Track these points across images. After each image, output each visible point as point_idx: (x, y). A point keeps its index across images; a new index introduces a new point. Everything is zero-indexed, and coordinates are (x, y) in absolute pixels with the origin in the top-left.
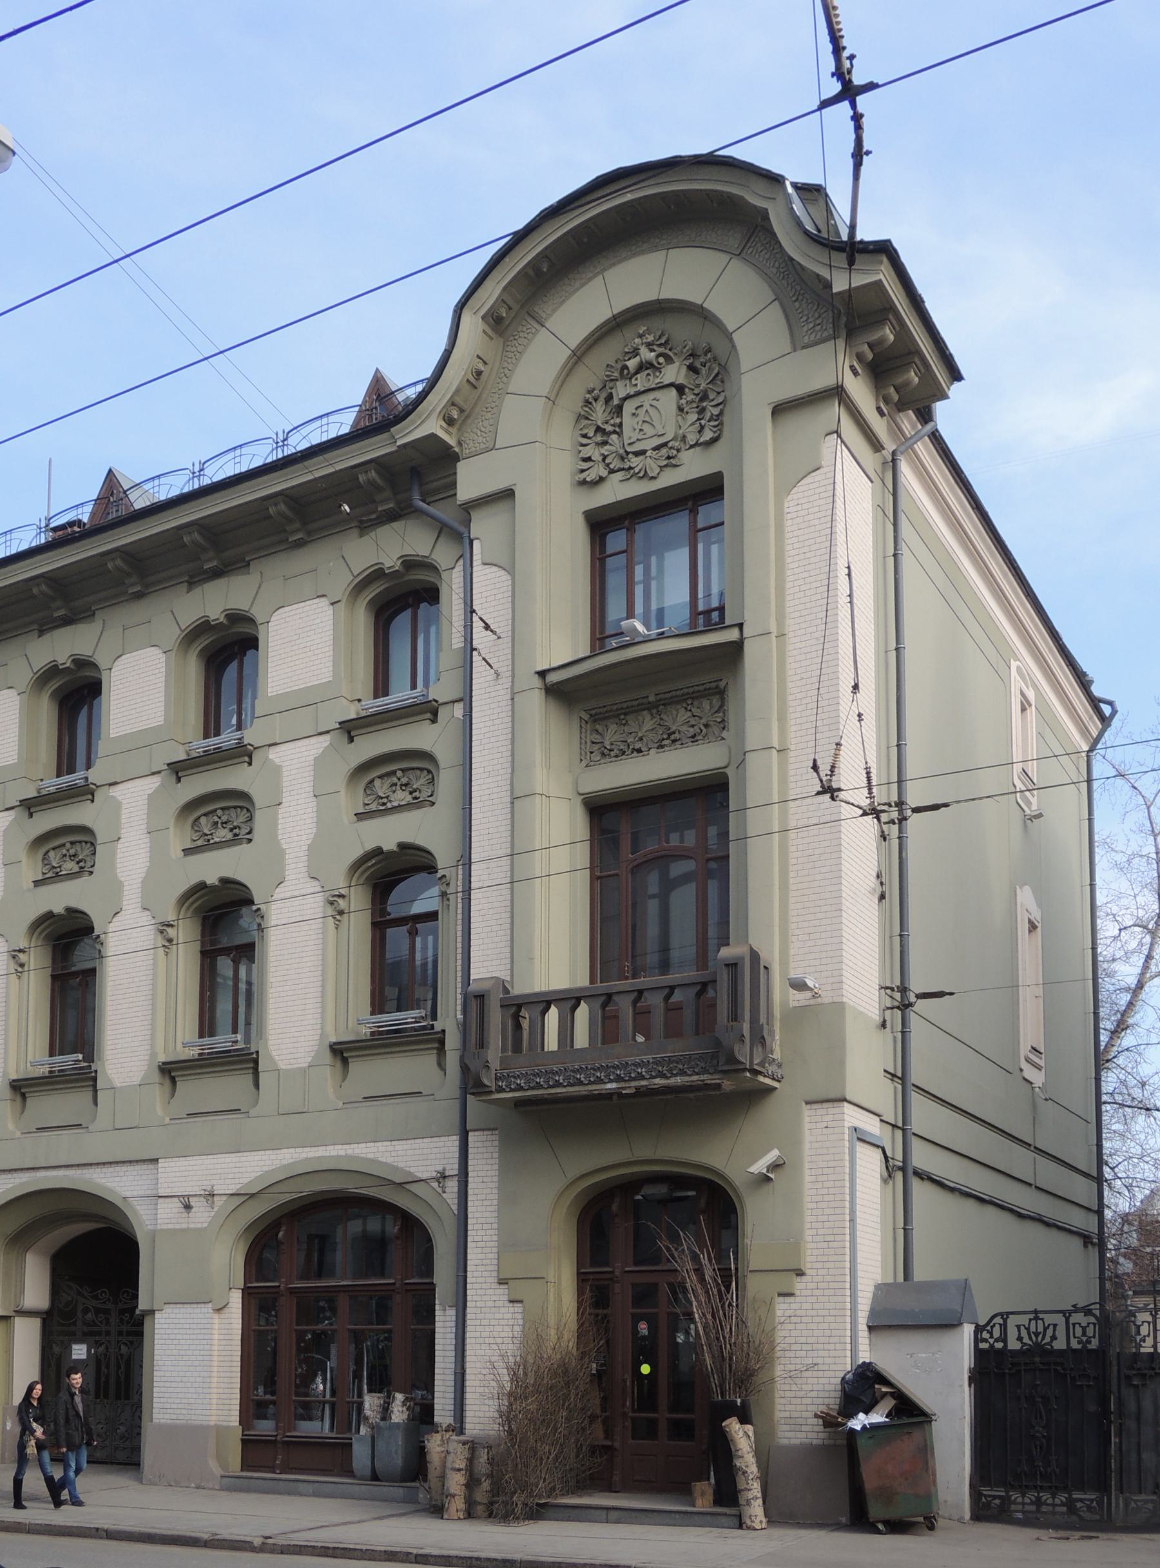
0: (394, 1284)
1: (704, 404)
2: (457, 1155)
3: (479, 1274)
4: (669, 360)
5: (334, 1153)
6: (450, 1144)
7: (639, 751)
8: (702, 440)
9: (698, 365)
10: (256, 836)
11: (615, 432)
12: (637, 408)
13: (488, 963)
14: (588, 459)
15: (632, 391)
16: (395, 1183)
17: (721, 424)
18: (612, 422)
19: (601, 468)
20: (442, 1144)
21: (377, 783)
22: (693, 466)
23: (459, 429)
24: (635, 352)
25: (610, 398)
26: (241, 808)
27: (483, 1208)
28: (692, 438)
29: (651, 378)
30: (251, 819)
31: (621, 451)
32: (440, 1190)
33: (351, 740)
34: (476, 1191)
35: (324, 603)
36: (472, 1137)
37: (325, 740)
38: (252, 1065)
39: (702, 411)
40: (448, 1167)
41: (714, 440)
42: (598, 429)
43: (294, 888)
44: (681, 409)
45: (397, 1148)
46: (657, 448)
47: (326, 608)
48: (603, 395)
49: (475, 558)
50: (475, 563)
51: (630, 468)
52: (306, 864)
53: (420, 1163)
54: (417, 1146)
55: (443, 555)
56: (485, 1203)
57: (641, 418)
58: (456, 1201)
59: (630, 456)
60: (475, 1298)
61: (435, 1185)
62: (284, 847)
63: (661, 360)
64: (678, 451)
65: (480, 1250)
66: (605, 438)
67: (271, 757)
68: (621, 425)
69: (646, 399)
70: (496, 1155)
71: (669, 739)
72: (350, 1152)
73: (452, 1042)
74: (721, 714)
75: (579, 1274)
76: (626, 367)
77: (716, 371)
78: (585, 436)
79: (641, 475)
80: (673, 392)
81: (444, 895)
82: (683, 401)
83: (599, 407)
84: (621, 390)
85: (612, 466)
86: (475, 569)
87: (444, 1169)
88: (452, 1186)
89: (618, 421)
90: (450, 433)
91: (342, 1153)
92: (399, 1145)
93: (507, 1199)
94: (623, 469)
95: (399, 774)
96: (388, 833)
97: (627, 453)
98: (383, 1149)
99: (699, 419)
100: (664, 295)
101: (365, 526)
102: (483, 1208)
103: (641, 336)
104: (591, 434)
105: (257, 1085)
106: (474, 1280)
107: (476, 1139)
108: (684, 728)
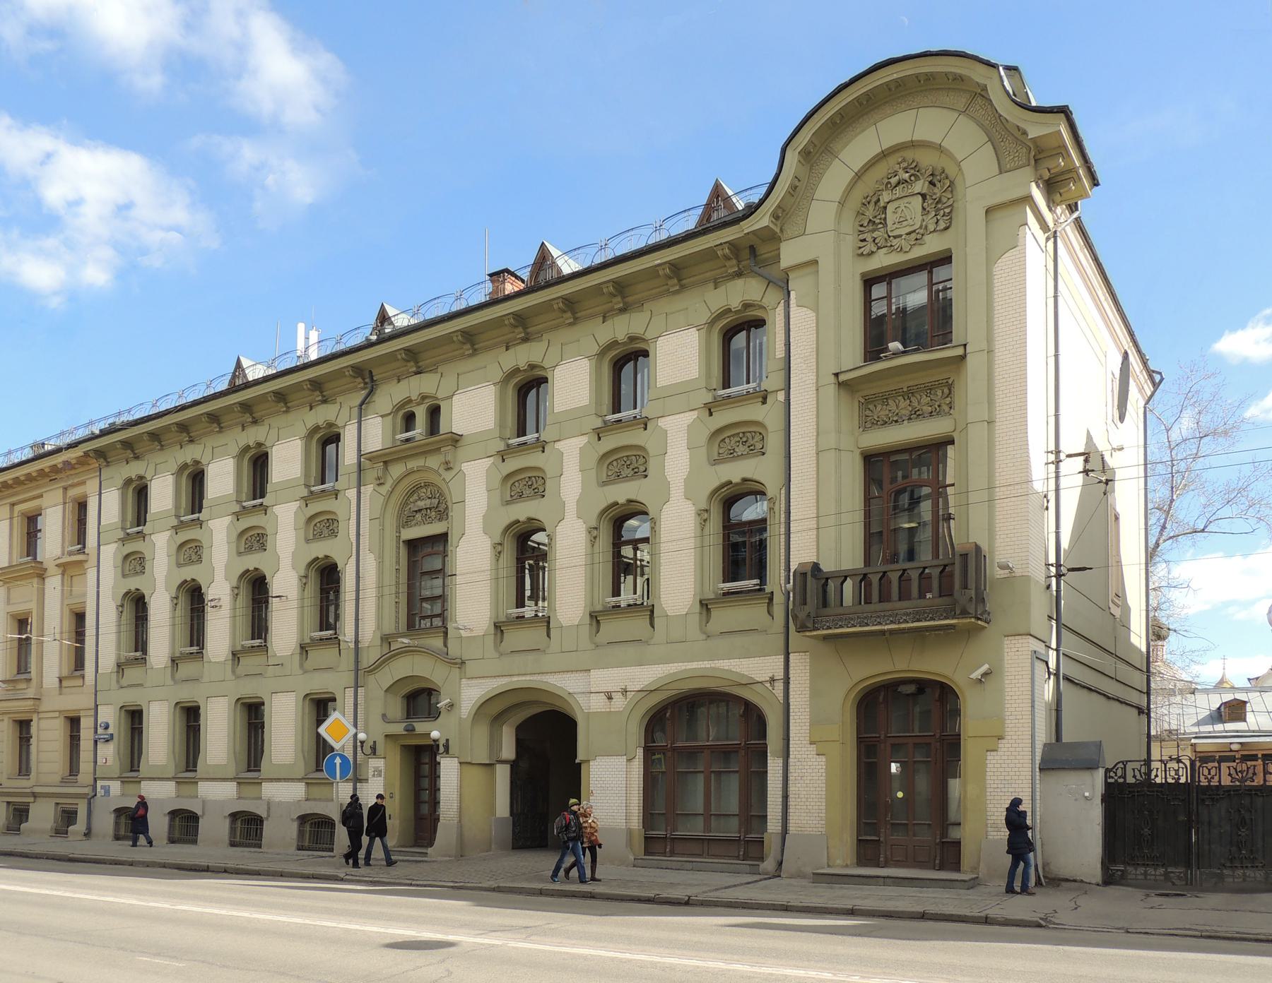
96: (735, 472)
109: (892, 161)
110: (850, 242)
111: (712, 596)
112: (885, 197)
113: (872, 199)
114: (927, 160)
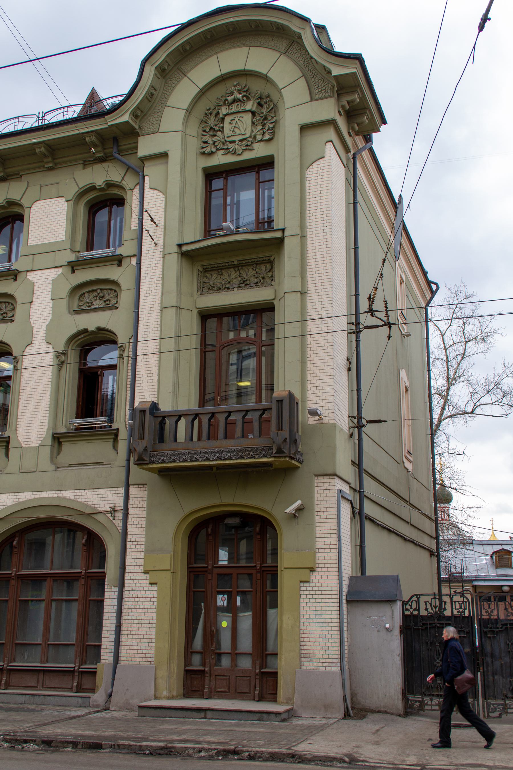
0: (81, 572)
1: (265, 122)
2: (123, 498)
3: (133, 567)
4: (249, 99)
5: (51, 496)
6: (119, 492)
7: (228, 288)
8: (264, 139)
9: (262, 103)
10: (17, 318)
11: (220, 131)
12: (232, 120)
13: (146, 393)
14: (206, 142)
15: (230, 112)
16: (85, 514)
17: (274, 132)
18: (219, 125)
19: (212, 147)
20: (114, 492)
21: (86, 295)
22: (260, 151)
23: (140, 121)
24: (232, 94)
25: (218, 113)
26: (9, 303)
27: (136, 529)
28: (259, 137)
29: (239, 107)
30: (14, 309)
31: (223, 140)
32: (111, 518)
33: (73, 272)
34: (133, 519)
35: (63, 200)
36: (132, 489)
37: (59, 271)
38: (5, 444)
39: (264, 125)
40: (117, 505)
41: (270, 140)
42: (211, 128)
43: (37, 347)
44: (253, 123)
45: (88, 493)
46: (241, 141)
47: (64, 203)
48: (215, 112)
49: (146, 185)
50: (145, 188)
51: (227, 149)
52: (45, 335)
53: (101, 502)
54: (99, 493)
55: (129, 182)
56: (138, 526)
57: (233, 125)
58: (121, 525)
59: (228, 143)
60: (130, 581)
61: (109, 515)
62: (33, 325)
63: (245, 98)
64: (252, 143)
65: (133, 553)
66: (215, 133)
67: (28, 277)
68: (223, 128)
69: (237, 117)
70: (145, 499)
71: (244, 284)
72: (60, 495)
73: (123, 435)
74: (271, 273)
75: (188, 568)
76: (227, 100)
77: (272, 106)
78: (204, 131)
79: (233, 152)
80: (250, 115)
81: (121, 356)
82: (255, 119)
83: (212, 118)
84: (224, 111)
85: (218, 147)
86: (145, 191)
87: (115, 506)
88: (120, 516)
89: (222, 125)
90: (135, 122)
91: (55, 495)
92: (89, 492)
93: (150, 524)
94: (224, 149)
95: (99, 291)
96: (91, 321)
97: (226, 141)
98: (80, 494)
99: (262, 129)
100: (249, 67)
101: (85, 164)
102: (136, 529)
103: (235, 86)
104: (208, 130)
105: (7, 455)
106: (129, 571)
107: (134, 489)
108: (252, 279)
109: (230, 86)
110: (194, 144)
111: (64, 430)
112: (224, 111)
113: (213, 112)
114: (257, 87)
